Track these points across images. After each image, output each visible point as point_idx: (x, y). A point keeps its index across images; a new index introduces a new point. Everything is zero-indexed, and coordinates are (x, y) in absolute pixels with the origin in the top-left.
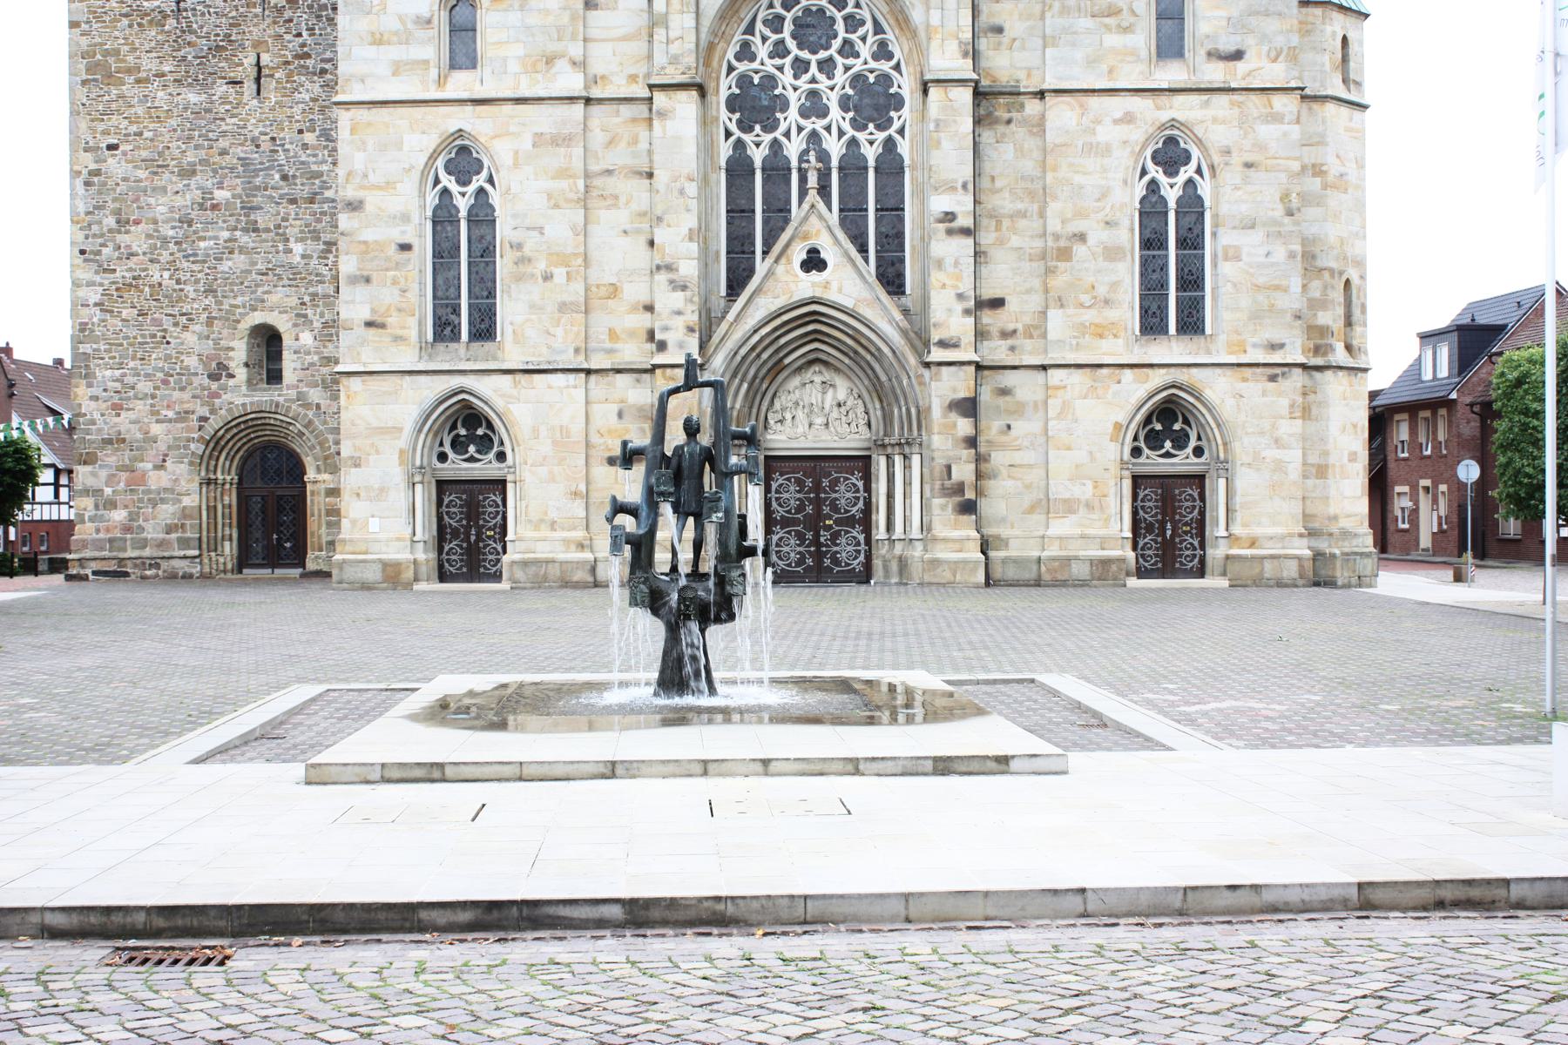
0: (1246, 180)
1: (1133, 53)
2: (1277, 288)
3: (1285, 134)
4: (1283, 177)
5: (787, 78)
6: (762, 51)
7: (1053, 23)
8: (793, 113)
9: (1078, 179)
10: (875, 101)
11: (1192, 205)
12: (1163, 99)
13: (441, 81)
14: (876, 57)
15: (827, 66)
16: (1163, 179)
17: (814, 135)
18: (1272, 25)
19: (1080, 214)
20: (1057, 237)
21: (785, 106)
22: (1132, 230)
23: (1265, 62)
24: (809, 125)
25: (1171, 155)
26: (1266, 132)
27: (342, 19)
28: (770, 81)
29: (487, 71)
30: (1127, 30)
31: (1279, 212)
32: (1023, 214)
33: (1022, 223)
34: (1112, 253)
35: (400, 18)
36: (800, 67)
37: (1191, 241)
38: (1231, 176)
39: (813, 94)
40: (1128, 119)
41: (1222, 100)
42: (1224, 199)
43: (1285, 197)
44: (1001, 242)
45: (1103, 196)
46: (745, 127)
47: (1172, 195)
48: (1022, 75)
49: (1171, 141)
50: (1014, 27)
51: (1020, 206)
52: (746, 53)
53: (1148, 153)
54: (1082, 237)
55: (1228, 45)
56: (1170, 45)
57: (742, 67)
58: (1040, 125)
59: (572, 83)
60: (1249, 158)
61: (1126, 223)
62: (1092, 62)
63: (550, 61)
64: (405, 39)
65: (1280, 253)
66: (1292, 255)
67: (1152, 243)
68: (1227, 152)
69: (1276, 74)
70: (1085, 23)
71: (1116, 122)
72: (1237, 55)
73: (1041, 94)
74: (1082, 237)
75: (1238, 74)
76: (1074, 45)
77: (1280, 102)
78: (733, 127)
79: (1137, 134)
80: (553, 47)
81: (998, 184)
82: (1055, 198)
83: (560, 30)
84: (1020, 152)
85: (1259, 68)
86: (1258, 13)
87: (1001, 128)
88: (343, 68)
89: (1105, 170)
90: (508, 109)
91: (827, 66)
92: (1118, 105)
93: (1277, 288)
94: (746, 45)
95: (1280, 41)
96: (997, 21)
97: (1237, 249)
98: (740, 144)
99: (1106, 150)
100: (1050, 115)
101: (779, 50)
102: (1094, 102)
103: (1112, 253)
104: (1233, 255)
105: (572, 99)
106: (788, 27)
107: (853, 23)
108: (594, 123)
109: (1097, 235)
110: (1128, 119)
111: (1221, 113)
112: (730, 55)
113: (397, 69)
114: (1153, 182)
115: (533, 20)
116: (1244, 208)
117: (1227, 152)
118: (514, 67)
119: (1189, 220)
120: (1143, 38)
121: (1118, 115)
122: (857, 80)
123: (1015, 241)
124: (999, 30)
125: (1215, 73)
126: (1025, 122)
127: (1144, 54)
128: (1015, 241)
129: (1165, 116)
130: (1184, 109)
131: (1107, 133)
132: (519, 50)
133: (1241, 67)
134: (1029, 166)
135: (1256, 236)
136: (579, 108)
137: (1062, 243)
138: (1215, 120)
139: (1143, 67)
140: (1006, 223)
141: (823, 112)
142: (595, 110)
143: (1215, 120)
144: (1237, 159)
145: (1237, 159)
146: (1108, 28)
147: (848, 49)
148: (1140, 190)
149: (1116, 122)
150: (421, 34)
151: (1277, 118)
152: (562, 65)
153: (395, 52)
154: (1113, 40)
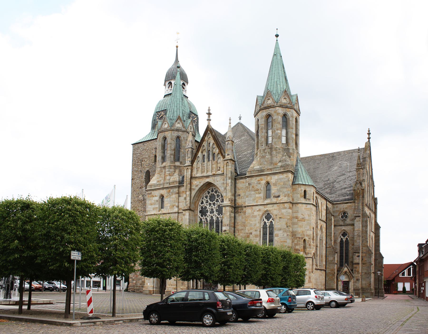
0: (280, 221)
1: (260, 197)
2: (285, 242)
3: (287, 211)
4: (286, 220)
5: (208, 207)
6: (204, 202)
7: (247, 193)
8: (208, 214)
9: (251, 222)
10: (220, 211)
11: (271, 226)
12: (266, 206)
13: (159, 211)
14: (222, 202)
15: (214, 204)
16: (266, 221)
17: (212, 217)
18: (285, 190)
19: (251, 229)
20: (247, 233)
21: (207, 211)
22: (260, 232)
23: (283, 197)
24: (211, 215)
25: (268, 217)
26: (284, 211)
27: (147, 202)
28: (206, 207)
29: (165, 209)
30: (260, 193)
31: (285, 227)
32: (242, 229)
33: (242, 231)
34: (256, 236)
35: (154, 201)
36: (210, 204)
37: (271, 233)
38: (277, 220)
39: (212, 209)
40: (259, 210)
41: (276, 205)
42: (276, 225)
43: (286, 224)
44: (239, 235)
45: (255, 225)
46: (202, 216)
47: (268, 224)
48: (243, 203)
49: (268, 214)
50: (242, 194)
51: (242, 228)
52: (202, 203)
53: (264, 217)
54: (251, 233)
55: (277, 195)
56: (268, 195)
57: (201, 205)
58: (245, 213)
59: (176, 210)
60: (280, 216)
61: (259, 230)
62: (254, 200)
63: (173, 206)
64: (155, 204)
65: (285, 235)
66: (288, 235)
67: (265, 234)
68: (276, 215)
69: (285, 199)
70: (253, 192)
71: (257, 211)
72: (279, 196)
73: (245, 207)
74: (251, 233)
75: (279, 200)
76: (251, 197)
77: (286, 205)
78: (200, 216)
79: (261, 213)
80: (174, 204)
81: (239, 224)
82: (247, 226)
83: (175, 201)
84: (242, 218)
85: (283, 199)
86: (282, 188)
87: (239, 214)
88: (147, 209)
89: (255, 220)
90: (167, 215)
91: (214, 204)
92: (257, 208)
93: (285, 242)
94: (202, 201)
95: (286, 193)
96: (239, 194)
97: (278, 234)
98: (201, 219)
99: (255, 217)
100: (247, 211)
101: (207, 202)
102: (254, 207)
103: (256, 236)
104: (277, 236)
105: (176, 213)
106: (208, 197)
107: (218, 196)
108: (179, 217)
109: (254, 233)
110: (259, 210)
111: (276, 208)
112: (200, 203)
113: (154, 209)
114: (265, 222)
115: (171, 199)
116: (279, 226)
117: (276, 215)
118: (168, 208)
119: (271, 229)
120: (262, 195)
121: (258, 210)
122: (219, 206)
123: (241, 235)
124: (239, 195)
125: (275, 200)
126: (243, 212)
127: (263, 198)
128: (241, 235)
129: (266, 209)
130: (269, 208)
131: (256, 213)
132: (169, 205)
133: (279, 198)
134: (243, 220)
135: (281, 232)
136: (177, 214)
137: (248, 235)
138: (274, 209)
139: (262, 200)
140: (240, 231)
141: (213, 212)
142: (180, 214)
143: (274, 209)
144: (278, 217)
145: (278, 217)
146: (257, 193)
147: (217, 201)
148: (262, 224)
149: (257, 211)
150: (157, 203)
151: (285, 208)
152: (175, 207)
153: (153, 206)
154: (257, 195)
